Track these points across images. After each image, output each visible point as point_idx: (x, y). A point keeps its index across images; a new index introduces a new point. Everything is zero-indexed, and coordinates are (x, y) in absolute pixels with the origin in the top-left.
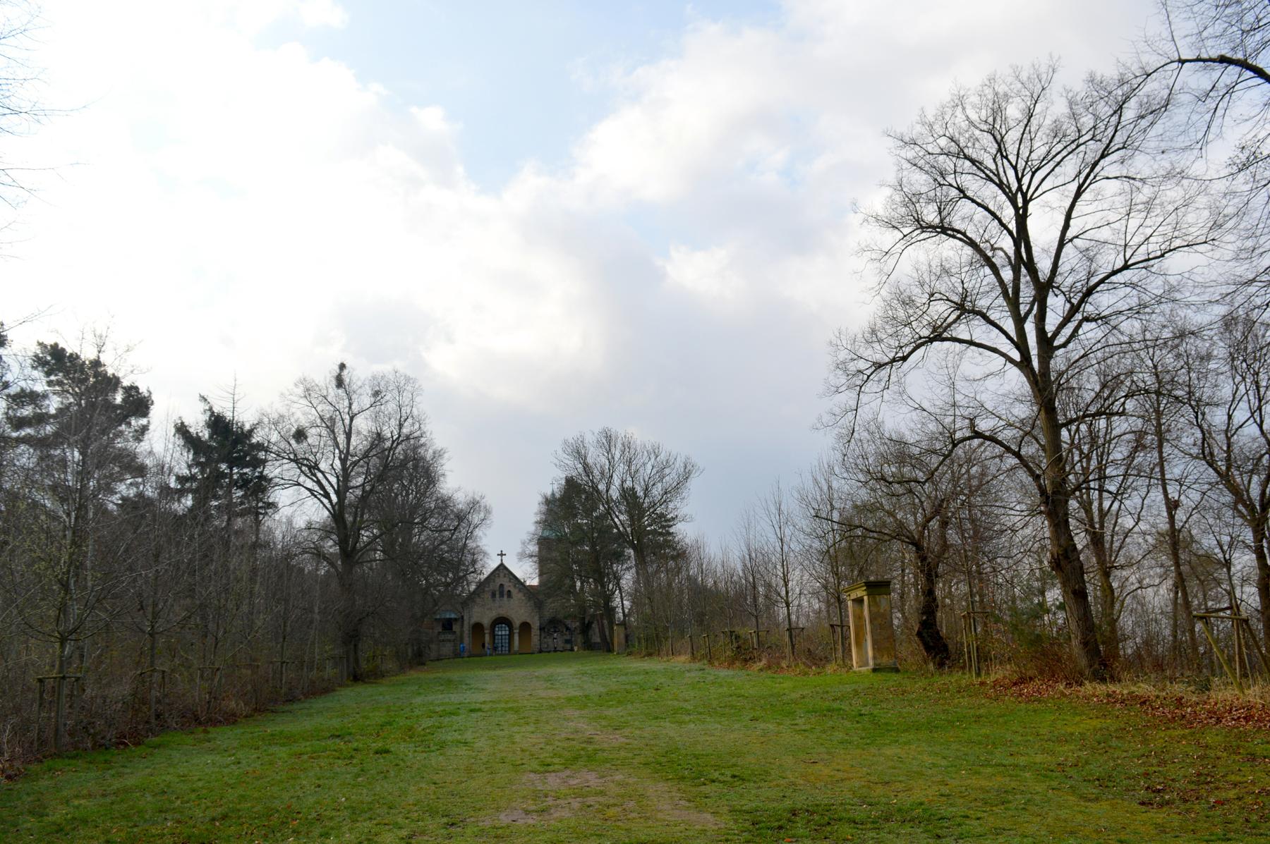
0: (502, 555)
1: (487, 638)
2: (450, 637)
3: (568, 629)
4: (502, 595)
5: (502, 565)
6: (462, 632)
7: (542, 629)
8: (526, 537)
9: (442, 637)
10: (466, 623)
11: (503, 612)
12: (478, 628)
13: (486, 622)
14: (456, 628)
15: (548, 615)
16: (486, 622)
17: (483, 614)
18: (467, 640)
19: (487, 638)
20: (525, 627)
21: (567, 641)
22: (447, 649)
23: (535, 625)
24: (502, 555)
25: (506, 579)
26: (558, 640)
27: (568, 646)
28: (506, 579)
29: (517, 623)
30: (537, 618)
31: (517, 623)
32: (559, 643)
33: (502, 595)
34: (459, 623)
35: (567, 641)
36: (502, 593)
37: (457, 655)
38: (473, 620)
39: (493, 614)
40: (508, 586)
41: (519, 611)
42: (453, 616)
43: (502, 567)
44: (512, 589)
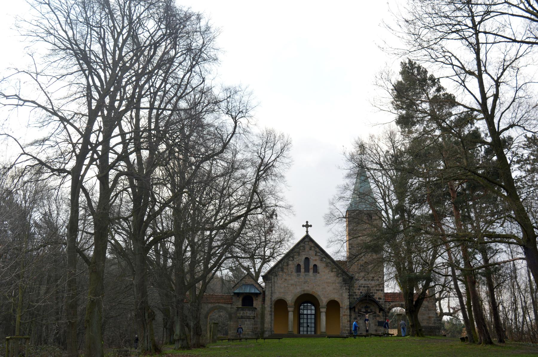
0: (307, 226)
1: (291, 316)
2: (248, 313)
3: (381, 309)
4: (307, 270)
5: (307, 239)
6: (263, 308)
7: (352, 308)
8: (334, 192)
9: (241, 313)
10: (267, 299)
11: (308, 288)
12: (280, 305)
13: (290, 299)
14: (257, 303)
15: (359, 292)
16: (290, 299)
17: (289, 289)
18: (268, 318)
19: (291, 316)
20: (333, 305)
21: (380, 324)
22: (247, 326)
23: (345, 303)
24: (307, 226)
25: (312, 252)
26: (370, 322)
27: (382, 330)
28: (312, 252)
29: (324, 301)
30: (346, 295)
31: (324, 301)
32: (372, 325)
33: (307, 270)
34: (260, 299)
35: (380, 324)
36: (307, 267)
37: (259, 335)
38: (276, 296)
39: (298, 291)
40: (314, 260)
42: (253, 291)
43: (307, 239)
44: (318, 263)
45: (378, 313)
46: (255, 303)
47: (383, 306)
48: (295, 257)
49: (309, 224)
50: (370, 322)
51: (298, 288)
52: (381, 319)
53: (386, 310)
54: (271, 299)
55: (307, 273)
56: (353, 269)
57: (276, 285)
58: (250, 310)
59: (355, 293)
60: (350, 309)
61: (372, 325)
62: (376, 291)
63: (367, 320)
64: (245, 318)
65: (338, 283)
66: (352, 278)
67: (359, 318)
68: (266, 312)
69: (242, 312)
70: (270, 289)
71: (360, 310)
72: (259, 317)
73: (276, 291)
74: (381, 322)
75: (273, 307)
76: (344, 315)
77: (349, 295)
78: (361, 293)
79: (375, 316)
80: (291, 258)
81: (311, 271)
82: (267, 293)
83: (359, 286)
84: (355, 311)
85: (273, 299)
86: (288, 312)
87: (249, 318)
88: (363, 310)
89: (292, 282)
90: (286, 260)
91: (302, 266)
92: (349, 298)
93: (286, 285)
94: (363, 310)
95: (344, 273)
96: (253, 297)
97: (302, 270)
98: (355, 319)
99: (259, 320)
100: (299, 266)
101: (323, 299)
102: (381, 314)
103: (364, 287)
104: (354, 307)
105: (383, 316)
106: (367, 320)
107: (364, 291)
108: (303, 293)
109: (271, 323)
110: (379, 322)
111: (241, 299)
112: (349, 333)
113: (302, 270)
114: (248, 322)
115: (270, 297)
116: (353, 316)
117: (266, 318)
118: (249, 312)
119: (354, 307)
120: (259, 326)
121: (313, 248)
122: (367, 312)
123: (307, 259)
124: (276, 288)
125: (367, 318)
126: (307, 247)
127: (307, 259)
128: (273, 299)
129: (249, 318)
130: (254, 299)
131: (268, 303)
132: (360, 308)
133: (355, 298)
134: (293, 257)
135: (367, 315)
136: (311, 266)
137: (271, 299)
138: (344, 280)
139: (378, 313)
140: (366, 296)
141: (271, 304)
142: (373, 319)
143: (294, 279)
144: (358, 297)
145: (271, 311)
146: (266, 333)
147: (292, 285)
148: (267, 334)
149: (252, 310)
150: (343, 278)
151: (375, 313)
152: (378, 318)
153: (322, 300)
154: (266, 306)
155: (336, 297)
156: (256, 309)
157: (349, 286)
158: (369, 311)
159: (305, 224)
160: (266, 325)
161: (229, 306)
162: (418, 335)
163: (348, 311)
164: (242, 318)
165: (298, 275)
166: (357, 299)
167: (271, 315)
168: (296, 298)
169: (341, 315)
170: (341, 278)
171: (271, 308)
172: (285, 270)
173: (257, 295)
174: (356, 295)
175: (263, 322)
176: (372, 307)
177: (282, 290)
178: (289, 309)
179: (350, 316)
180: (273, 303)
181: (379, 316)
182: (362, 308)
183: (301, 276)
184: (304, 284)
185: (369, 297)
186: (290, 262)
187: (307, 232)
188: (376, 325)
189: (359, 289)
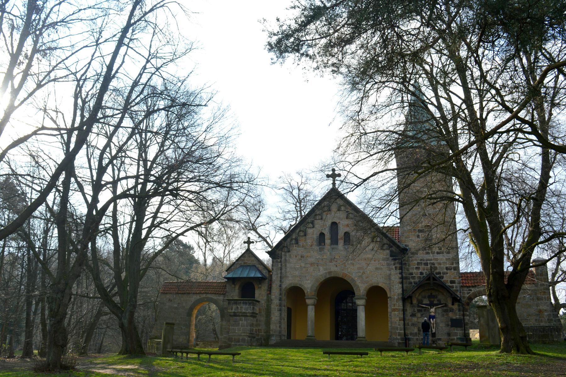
2: (245, 308)
3: (455, 300)
4: (334, 241)
6: (269, 301)
7: (406, 299)
10: (275, 286)
11: (336, 269)
12: (296, 294)
13: (309, 285)
14: (260, 293)
15: (417, 272)
16: (309, 285)
20: (377, 295)
23: (395, 291)
24: (334, 176)
28: (342, 215)
30: (396, 277)
33: (334, 241)
34: (265, 287)
38: (288, 282)
39: (321, 273)
41: (368, 269)
42: (252, 275)
45: (450, 305)
46: (257, 292)
47: (458, 294)
48: (316, 222)
49: (336, 172)
50: (438, 321)
51: (321, 268)
52: (456, 316)
53: (464, 300)
54: (280, 286)
55: (335, 246)
56: (412, 242)
57: (288, 265)
58: (246, 304)
59: (412, 274)
60: (404, 300)
61: (442, 325)
62: (445, 271)
63: (433, 317)
64: (239, 316)
65: (384, 260)
66: (404, 251)
67: (419, 315)
68: (272, 306)
69: (234, 307)
70: (279, 272)
71: (420, 302)
72: (263, 313)
73: (288, 274)
74: (456, 320)
75: (284, 298)
76: (394, 310)
77: (402, 278)
78: (421, 273)
79: (446, 311)
80: (311, 225)
81: (341, 243)
82: (274, 278)
83: (418, 264)
84: (411, 303)
85: (284, 286)
86: (306, 306)
87: (245, 315)
88: (426, 301)
89: (312, 260)
90: (302, 228)
91: (327, 236)
92: (402, 283)
93: (303, 265)
94: (426, 301)
95: (392, 243)
96: (254, 284)
97: (328, 241)
98: (413, 315)
99: (263, 319)
100: (322, 235)
101: (360, 285)
102: (456, 307)
103: (426, 264)
104: (410, 297)
105: (459, 310)
106: (433, 317)
107: (425, 269)
108: (328, 276)
109: (280, 322)
110: (452, 320)
111: (237, 287)
112: (402, 339)
113: (328, 241)
114: (243, 322)
115: (279, 283)
116: (409, 311)
117: (272, 316)
118: (244, 306)
119: (410, 297)
120: (263, 327)
121: (343, 208)
122: (432, 305)
123: (334, 225)
124: (288, 269)
125: (433, 314)
126: (334, 207)
127: (334, 225)
128: (284, 286)
129: (245, 315)
130: (256, 287)
131: (275, 292)
132: (420, 298)
133: (411, 283)
134: (312, 223)
135: (433, 310)
136: (341, 234)
137: (280, 286)
138: (392, 255)
139: (450, 305)
140: (428, 279)
141: (280, 294)
142: (443, 315)
143: (314, 255)
144: (417, 280)
145: (280, 305)
146: (273, 338)
147: (312, 264)
148: (274, 340)
149: (250, 304)
150: (391, 252)
151: (446, 305)
152: (451, 314)
153: (358, 287)
154: (273, 297)
155: (379, 280)
156: (258, 302)
157: (401, 263)
158: (435, 302)
159: (330, 173)
160: (272, 327)
161: (221, 298)
162: (518, 350)
163: (401, 303)
164: (235, 315)
165: (321, 250)
166: (415, 283)
167: (280, 310)
168: (317, 284)
169: (389, 310)
170: (388, 252)
171: (280, 299)
172: (301, 243)
173: (260, 280)
174: (413, 278)
175: (268, 322)
176: (440, 297)
177: (297, 273)
178: (308, 301)
179: (404, 311)
180: (284, 292)
181: (452, 310)
182: (425, 297)
183: (326, 251)
184: (331, 262)
185: (434, 279)
186: (310, 231)
187: (334, 184)
188: (448, 325)
189: (418, 268)
